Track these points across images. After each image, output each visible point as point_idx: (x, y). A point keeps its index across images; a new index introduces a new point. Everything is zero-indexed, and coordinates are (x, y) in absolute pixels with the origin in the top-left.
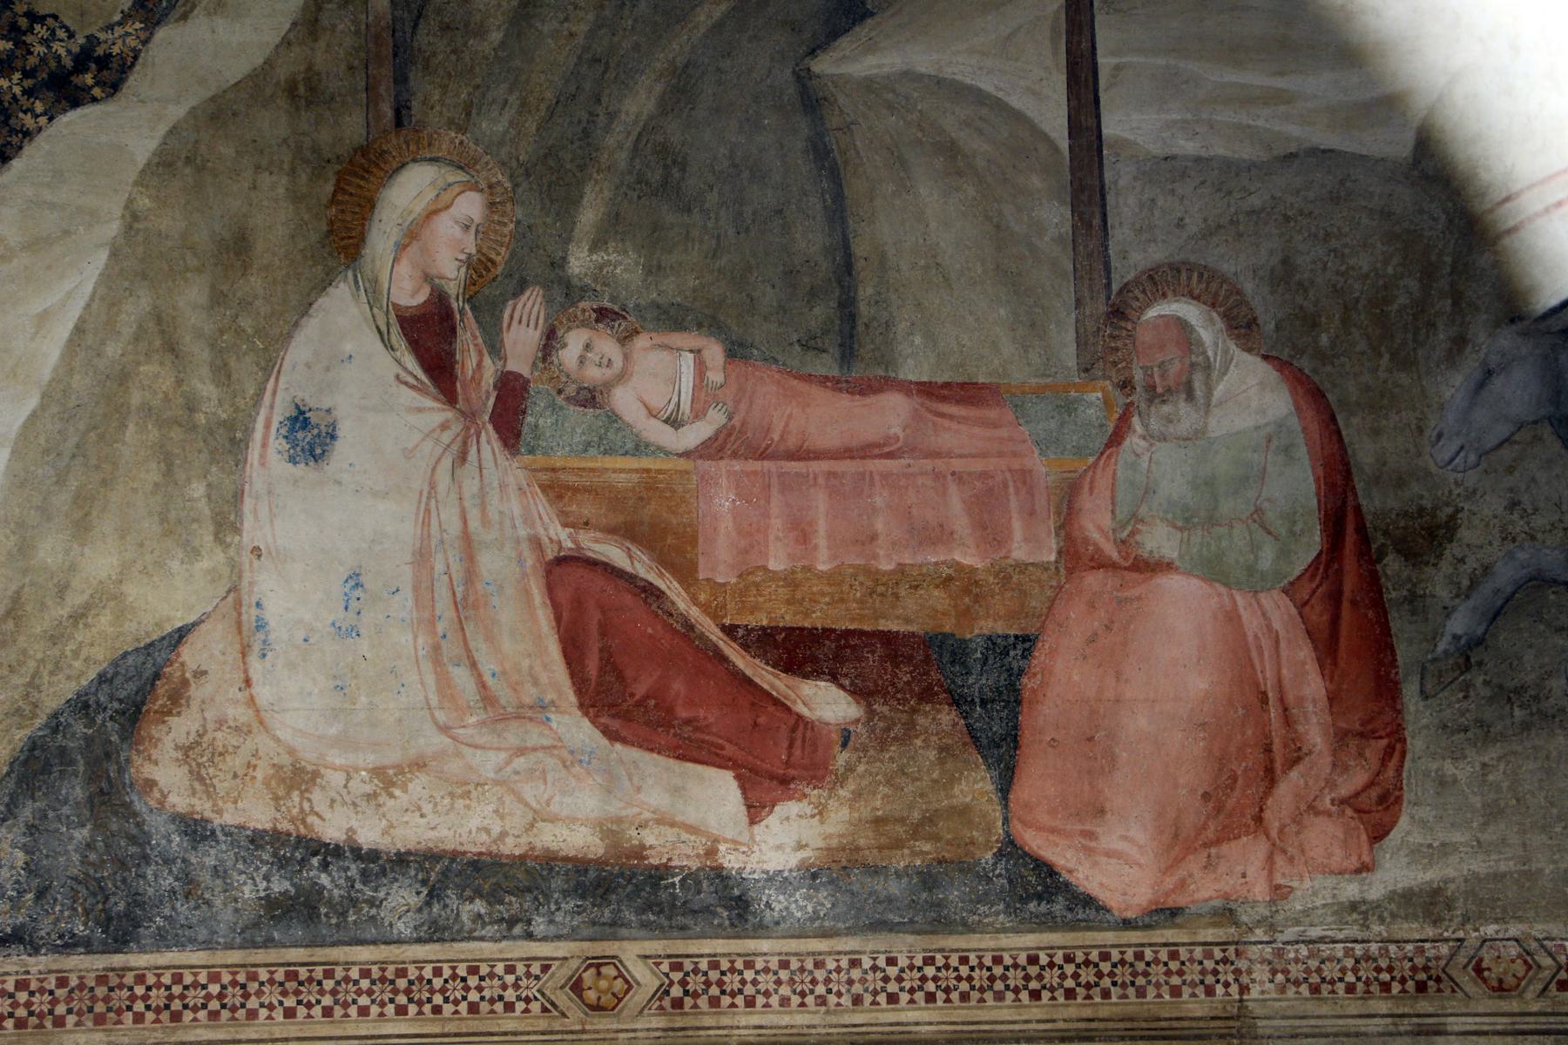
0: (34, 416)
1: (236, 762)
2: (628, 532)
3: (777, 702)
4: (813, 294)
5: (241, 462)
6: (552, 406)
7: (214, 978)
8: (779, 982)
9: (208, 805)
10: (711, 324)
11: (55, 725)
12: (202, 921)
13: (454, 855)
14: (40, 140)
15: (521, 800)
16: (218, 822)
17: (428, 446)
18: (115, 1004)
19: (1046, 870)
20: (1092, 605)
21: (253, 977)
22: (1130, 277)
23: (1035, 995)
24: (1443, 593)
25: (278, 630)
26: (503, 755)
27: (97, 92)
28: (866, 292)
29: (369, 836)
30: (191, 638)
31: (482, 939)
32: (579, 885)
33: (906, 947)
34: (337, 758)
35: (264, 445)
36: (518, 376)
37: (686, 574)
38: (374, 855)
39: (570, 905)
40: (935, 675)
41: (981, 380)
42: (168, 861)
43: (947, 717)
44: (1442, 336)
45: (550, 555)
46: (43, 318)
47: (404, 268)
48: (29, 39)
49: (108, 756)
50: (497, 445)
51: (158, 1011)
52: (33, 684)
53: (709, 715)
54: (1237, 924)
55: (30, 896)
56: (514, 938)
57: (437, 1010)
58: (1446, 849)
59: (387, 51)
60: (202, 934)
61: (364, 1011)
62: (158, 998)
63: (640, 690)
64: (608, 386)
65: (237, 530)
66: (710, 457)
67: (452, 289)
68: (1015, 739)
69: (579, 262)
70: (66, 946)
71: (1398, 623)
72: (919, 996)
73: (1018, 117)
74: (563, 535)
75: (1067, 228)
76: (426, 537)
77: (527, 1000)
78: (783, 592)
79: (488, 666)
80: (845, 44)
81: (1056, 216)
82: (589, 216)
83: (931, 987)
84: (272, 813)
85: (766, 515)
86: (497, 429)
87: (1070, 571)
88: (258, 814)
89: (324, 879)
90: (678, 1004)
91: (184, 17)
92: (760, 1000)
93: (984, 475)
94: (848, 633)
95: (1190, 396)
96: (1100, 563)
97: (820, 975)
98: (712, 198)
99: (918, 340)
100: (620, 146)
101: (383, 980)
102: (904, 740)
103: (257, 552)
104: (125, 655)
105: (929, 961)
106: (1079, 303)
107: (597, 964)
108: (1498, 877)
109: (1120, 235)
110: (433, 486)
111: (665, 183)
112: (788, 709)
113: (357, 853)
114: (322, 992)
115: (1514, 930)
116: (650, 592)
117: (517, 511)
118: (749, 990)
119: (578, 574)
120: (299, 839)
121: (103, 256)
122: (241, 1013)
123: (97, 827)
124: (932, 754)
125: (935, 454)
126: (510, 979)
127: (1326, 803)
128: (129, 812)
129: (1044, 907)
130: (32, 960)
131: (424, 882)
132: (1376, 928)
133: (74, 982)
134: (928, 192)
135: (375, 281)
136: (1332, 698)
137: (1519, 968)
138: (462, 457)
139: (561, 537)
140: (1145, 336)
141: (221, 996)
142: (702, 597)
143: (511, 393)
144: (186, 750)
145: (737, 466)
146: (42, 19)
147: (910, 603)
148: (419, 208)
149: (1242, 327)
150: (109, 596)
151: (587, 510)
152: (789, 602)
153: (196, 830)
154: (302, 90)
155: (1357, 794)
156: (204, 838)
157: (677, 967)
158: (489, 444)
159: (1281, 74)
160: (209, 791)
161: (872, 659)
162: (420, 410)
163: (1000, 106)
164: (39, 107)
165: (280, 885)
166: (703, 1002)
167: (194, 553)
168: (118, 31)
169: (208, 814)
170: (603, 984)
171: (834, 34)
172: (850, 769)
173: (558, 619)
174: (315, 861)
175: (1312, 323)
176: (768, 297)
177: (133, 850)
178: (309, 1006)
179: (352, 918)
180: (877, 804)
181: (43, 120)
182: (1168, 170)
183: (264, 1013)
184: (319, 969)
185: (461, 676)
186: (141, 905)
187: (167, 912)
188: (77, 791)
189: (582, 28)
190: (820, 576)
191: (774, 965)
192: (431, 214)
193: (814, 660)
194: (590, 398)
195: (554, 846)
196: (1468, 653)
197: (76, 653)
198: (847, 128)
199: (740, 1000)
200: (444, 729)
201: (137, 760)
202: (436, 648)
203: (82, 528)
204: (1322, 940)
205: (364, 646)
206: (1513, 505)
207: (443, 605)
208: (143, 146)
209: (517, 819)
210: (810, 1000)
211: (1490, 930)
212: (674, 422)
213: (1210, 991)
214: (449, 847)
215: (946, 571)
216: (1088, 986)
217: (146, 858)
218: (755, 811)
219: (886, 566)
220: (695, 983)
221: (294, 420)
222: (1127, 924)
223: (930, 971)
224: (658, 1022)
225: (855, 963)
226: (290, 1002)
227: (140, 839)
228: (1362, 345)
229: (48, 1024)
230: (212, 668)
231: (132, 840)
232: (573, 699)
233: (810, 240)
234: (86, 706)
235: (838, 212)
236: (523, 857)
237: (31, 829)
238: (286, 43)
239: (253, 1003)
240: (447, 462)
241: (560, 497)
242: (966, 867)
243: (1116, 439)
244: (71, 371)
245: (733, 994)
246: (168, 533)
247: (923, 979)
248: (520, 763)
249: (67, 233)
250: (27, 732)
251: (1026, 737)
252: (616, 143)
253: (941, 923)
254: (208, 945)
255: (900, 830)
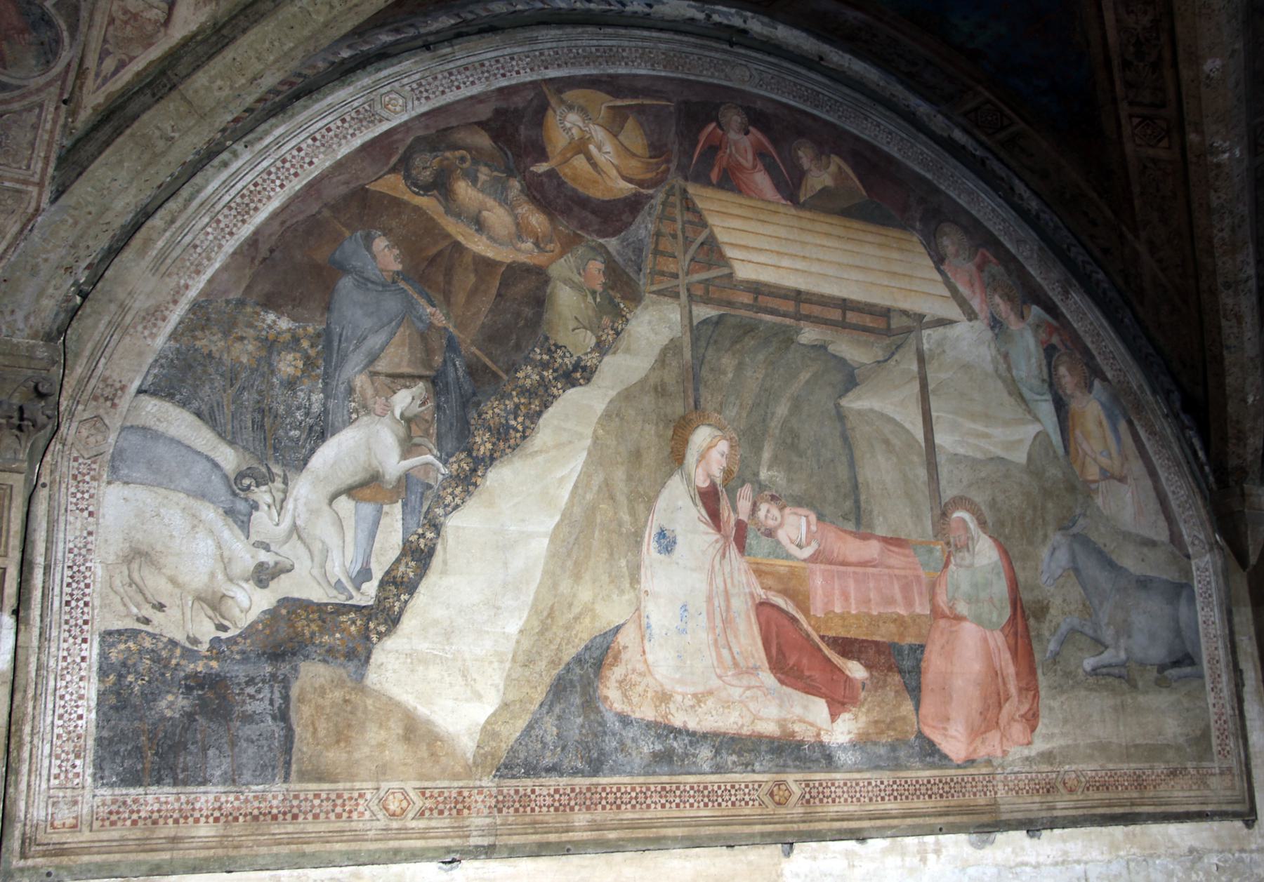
0: (558, 525)
1: (640, 689)
2: (785, 593)
3: (840, 670)
4: (845, 496)
5: (640, 552)
6: (756, 536)
7: (633, 789)
8: (843, 792)
9: (629, 709)
10: (810, 505)
11: (568, 669)
12: (628, 763)
13: (725, 734)
14: (559, 400)
15: (749, 710)
16: (633, 716)
17: (711, 549)
18: (594, 801)
19: (932, 744)
20: (942, 633)
21: (648, 789)
22: (947, 500)
23: (930, 797)
24: (1047, 634)
25: (655, 629)
26: (742, 690)
27: (581, 381)
28: (863, 498)
29: (692, 726)
30: (621, 631)
31: (735, 772)
32: (771, 748)
33: (887, 776)
34: (679, 689)
35: (649, 544)
36: (744, 522)
37: (806, 612)
38: (693, 734)
39: (768, 757)
40: (893, 660)
41: (903, 537)
42: (614, 734)
43: (897, 678)
44: (1040, 533)
45: (757, 601)
46: (562, 479)
47: (700, 470)
48: (555, 355)
49: (589, 684)
50: (736, 551)
51: (611, 804)
52: (559, 649)
53: (816, 674)
54: (992, 766)
55: (559, 749)
56: (748, 772)
57: (720, 805)
58: (1052, 736)
59: (691, 376)
60: (628, 769)
61: (692, 805)
62: (611, 798)
63: (791, 662)
64: (776, 528)
65: (639, 582)
66: (813, 562)
67: (718, 481)
68: (919, 688)
69: (764, 474)
70: (574, 773)
71: (1035, 645)
72: (892, 797)
73: (908, 431)
74: (761, 592)
75: (926, 478)
76: (711, 590)
77: (754, 800)
78: (840, 622)
79: (736, 649)
80: (850, 395)
81: (922, 473)
82: (766, 455)
83: (895, 793)
84: (654, 713)
85: (833, 589)
86: (736, 544)
87: (935, 619)
88: (648, 713)
89: (675, 744)
90: (808, 802)
91: (614, 353)
92: (837, 800)
93: (906, 577)
94: (863, 641)
95: (968, 550)
96: (944, 616)
97: (858, 789)
98: (809, 452)
99: (881, 519)
100: (776, 427)
101: (699, 791)
102: (883, 687)
103: (646, 592)
104: (596, 637)
105: (895, 782)
106: (932, 508)
107: (779, 784)
108: (1068, 746)
109: (943, 483)
110: (713, 567)
111: (792, 444)
112: (843, 673)
113: (688, 733)
114: (675, 796)
115: (1074, 767)
116: (794, 620)
117: (745, 581)
118: (833, 795)
119: (767, 610)
120: (665, 725)
121: (585, 454)
122: (644, 806)
123: (585, 717)
124: (893, 694)
125: (889, 567)
126: (747, 791)
127: (1017, 717)
128: (598, 711)
129: (931, 760)
130: (560, 779)
131: (713, 746)
132: (1034, 767)
133: (577, 790)
134: (881, 458)
135: (689, 475)
136: (1017, 674)
137: (1076, 782)
138: (724, 556)
139: (761, 593)
140: (953, 525)
141: (636, 798)
142: (813, 623)
143: (741, 527)
144: (620, 682)
145: (823, 566)
146: (560, 347)
147: (883, 630)
148: (705, 445)
149: (982, 524)
150: (589, 610)
151: (770, 581)
152: (843, 626)
153: (625, 720)
154: (659, 389)
155: (1026, 713)
156: (628, 724)
157: (807, 785)
158: (733, 550)
159: (987, 427)
160: (630, 704)
161: (871, 652)
162: (707, 533)
163: (903, 427)
164: (559, 385)
165: (658, 747)
166: (817, 801)
167: (622, 592)
168: (589, 356)
169: (630, 713)
170: (781, 793)
171: (847, 390)
172: (865, 700)
173: (761, 629)
174: (672, 736)
175: (1002, 524)
176: (831, 496)
177: (600, 729)
178: (671, 803)
179: (686, 762)
180: (875, 715)
181: (561, 391)
182: (956, 459)
183: (653, 806)
184: (674, 786)
185: (725, 652)
186: (604, 755)
187: (614, 758)
188: (577, 700)
189: (760, 376)
190: (853, 615)
191: (842, 784)
192: (710, 448)
193: (851, 652)
194: (770, 533)
195: (762, 731)
196: (1056, 656)
197: (576, 636)
198: (853, 429)
199: (830, 800)
200: (720, 677)
201: (601, 687)
202: (716, 641)
203: (577, 577)
204: (1018, 772)
205: (688, 638)
206: (1064, 600)
207: (718, 622)
208: (600, 407)
209: (747, 720)
210: (854, 799)
211: (1067, 767)
212: (800, 546)
213: (985, 794)
214: (723, 730)
215: (895, 616)
216: (947, 793)
217: (605, 733)
218: (834, 716)
219: (875, 613)
220: (814, 792)
221: (660, 534)
222: (959, 767)
223: (895, 787)
224: (801, 810)
225: (869, 784)
226: (663, 801)
227: (602, 724)
228: (1018, 535)
229: (568, 810)
230: (630, 645)
231: (600, 724)
232: (767, 665)
233: (843, 472)
234: (580, 660)
235: (852, 464)
236: (750, 736)
237: (559, 718)
238: (653, 369)
239: (649, 801)
240: (718, 558)
241: (760, 576)
242: (905, 742)
243: (946, 565)
244: (573, 506)
245: (828, 798)
246: (612, 582)
247: (893, 790)
248: (748, 693)
249: (570, 442)
250: (557, 671)
251: (923, 687)
252: (774, 424)
253: (898, 766)
254: (631, 774)
255: (883, 726)
